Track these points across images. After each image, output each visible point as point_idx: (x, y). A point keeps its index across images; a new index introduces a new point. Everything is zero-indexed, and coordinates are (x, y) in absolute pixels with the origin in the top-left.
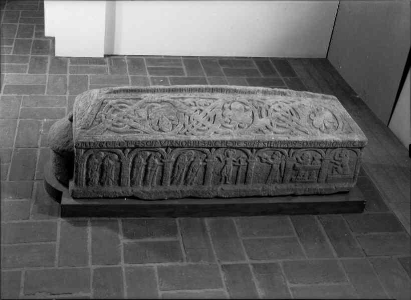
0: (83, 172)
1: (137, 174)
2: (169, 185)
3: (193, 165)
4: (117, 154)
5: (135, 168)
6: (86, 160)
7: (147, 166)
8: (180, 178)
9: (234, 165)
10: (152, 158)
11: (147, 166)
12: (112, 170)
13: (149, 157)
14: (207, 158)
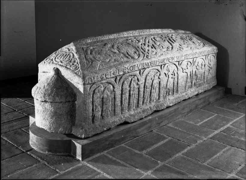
0: (90, 109)
1: (125, 99)
2: (142, 106)
3: (154, 83)
4: (111, 84)
5: (123, 94)
6: (92, 96)
7: (130, 91)
8: (148, 97)
9: (172, 78)
10: (133, 82)
11: (130, 91)
12: (109, 102)
13: (131, 82)
14: (160, 75)
